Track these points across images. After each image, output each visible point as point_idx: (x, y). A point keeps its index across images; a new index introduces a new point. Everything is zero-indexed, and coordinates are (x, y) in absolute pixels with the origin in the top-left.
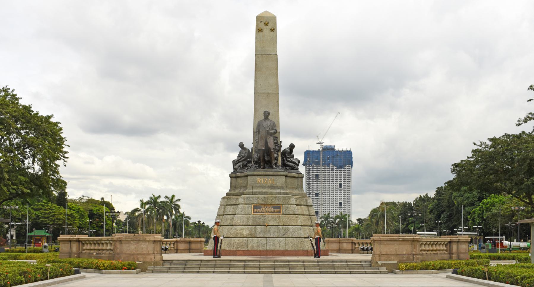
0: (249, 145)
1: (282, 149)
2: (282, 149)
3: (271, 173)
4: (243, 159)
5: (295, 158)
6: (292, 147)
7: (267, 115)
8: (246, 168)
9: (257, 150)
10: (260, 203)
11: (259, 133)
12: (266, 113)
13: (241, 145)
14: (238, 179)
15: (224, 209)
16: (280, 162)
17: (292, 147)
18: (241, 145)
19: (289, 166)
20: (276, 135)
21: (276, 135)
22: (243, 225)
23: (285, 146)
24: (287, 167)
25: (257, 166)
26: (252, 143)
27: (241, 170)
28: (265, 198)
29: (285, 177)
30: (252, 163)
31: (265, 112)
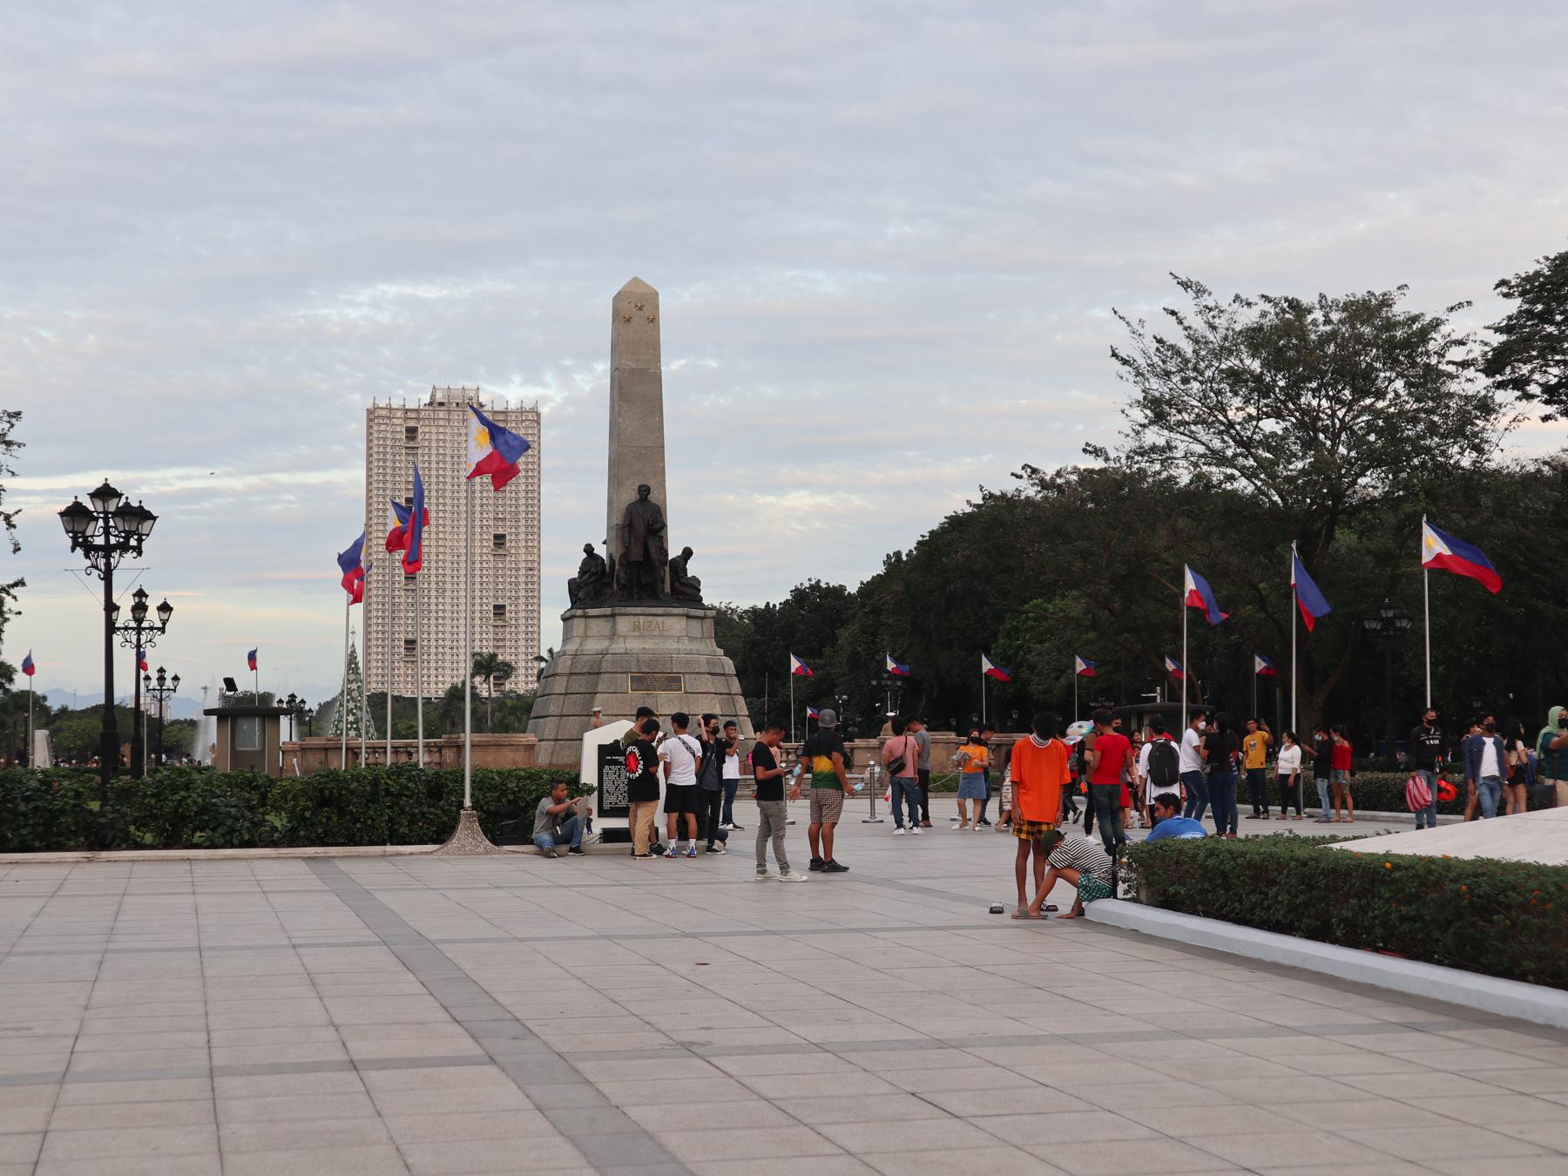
0: (601, 551)
1: (670, 557)
2: (670, 557)
3: (660, 610)
4: (593, 578)
5: (689, 576)
6: (688, 553)
7: (644, 491)
8: (603, 598)
9: (624, 562)
10: (643, 670)
11: (630, 532)
12: (644, 489)
13: (589, 549)
14: (588, 620)
15: (568, 681)
16: (668, 589)
17: (688, 553)
18: (589, 549)
19: (683, 593)
20: (661, 534)
21: (661, 534)
22: (612, 715)
23: (674, 551)
24: (681, 597)
25: (625, 594)
26: (604, 543)
27: (592, 602)
28: (651, 660)
29: (685, 618)
30: (612, 586)
31: (640, 487)
